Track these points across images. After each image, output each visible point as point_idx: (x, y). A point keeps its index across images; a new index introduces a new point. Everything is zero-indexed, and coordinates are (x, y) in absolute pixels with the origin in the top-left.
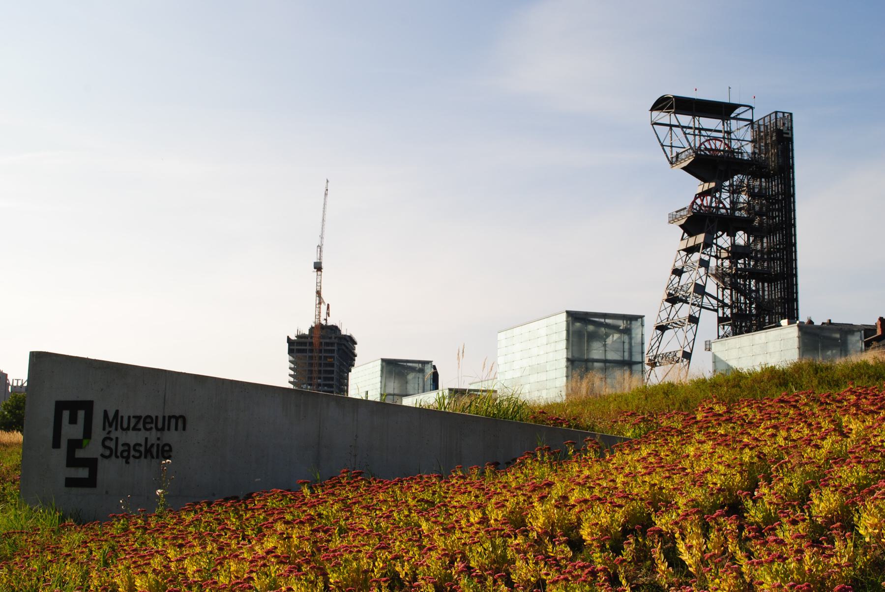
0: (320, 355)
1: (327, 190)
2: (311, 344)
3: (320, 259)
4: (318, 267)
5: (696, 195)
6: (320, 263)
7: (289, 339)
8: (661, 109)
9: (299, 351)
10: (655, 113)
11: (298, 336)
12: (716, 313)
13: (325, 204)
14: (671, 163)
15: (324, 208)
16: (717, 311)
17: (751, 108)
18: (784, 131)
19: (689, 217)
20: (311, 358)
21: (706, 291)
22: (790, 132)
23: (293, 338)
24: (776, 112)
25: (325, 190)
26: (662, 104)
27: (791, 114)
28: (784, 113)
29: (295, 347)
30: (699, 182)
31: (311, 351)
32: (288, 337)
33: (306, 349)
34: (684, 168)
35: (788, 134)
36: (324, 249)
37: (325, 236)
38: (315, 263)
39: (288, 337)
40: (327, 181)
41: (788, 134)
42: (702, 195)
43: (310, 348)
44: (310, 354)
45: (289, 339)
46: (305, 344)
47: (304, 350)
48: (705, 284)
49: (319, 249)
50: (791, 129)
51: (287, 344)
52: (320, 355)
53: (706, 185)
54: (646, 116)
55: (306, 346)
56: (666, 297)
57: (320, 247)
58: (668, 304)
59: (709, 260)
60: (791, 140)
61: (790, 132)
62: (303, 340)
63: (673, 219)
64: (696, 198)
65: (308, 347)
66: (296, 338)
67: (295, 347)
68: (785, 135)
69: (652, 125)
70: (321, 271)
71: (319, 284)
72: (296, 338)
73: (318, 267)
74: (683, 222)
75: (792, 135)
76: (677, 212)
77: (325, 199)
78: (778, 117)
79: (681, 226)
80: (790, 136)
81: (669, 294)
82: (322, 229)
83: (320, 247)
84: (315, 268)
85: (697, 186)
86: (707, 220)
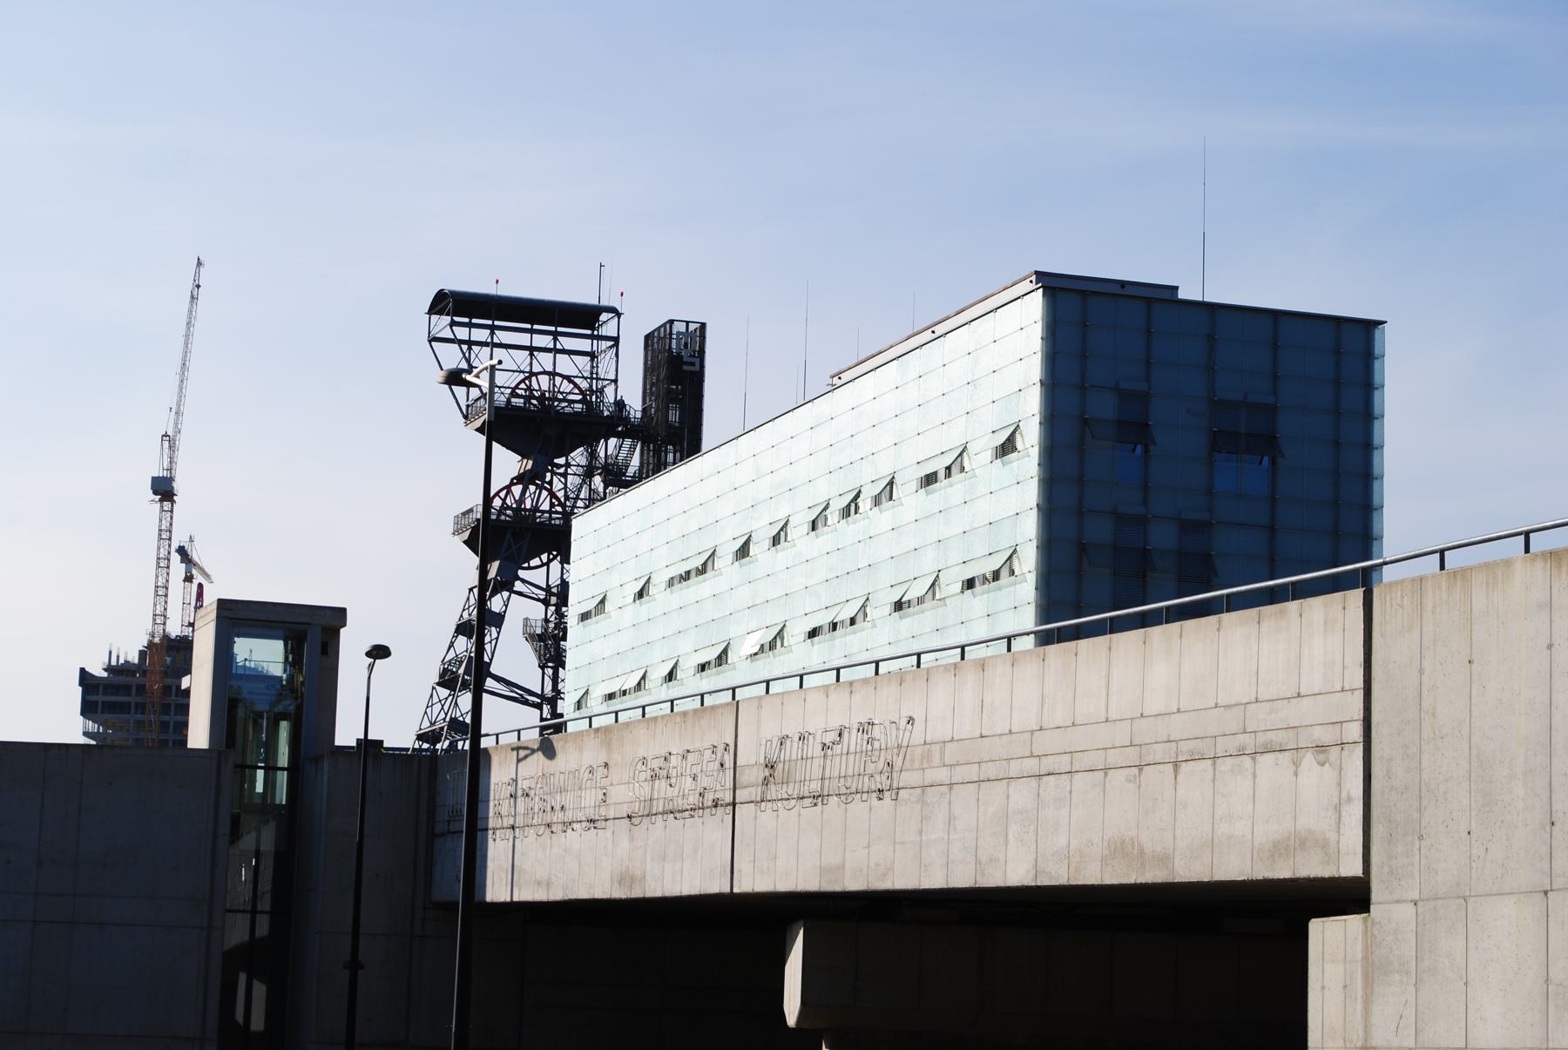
0: (166, 718)
1: (198, 286)
2: (141, 689)
3: (170, 470)
4: (164, 490)
5: (512, 479)
6: (171, 480)
7: (84, 676)
8: (440, 313)
9: (111, 707)
10: (435, 318)
11: (109, 669)
12: (539, 712)
13: (189, 324)
14: (466, 417)
15: (187, 336)
16: (539, 706)
17: (619, 315)
18: (685, 359)
19: (472, 528)
20: (140, 724)
21: (493, 670)
22: (697, 361)
23: (98, 671)
24: (671, 322)
25: (190, 285)
26: (448, 303)
27: (703, 326)
28: (687, 323)
29: (100, 698)
30: (520, 458)
31: (141, 707)
32: (83, 671)
33: (130, 703)
34: (477, 430)
35: (693, 364)
36: (183, 443)
37: (187, 410)
38: (154, 479)
39: (83, 671)
40: (199, 264)
41: (693, 364)
42: (523, 479)
43: (139, 699)
44: (139, 717)
45: (84, 676)
46: (126, 689)
47: (122, 704)
48: (491, 660)
49: (166, 444)
50: (702, 352)
51: (80, 688)
52: (166, 718)
53: (525, 461)
54: (418, 320)
55: (129, 695)
56: (437, 681)
57: (170, 440)
58: (444, 692)
59: (505, 612)
60: (698, 378)
61: (697, 361)
62: (122, 679)
63: (457, 532)
64: (512, 484)
65: (132, 699)
66: (105, 674)
67: (100, 698)
68: (685, 368)
69: (430, 341)
70: (173, 502)
71: (165, 534)
72: (105, 674)
73: (164, 490)
74: (466, 535)
75: (702, 366)
76: (464, 514)
77: (190, 312)
78: (674, 331)
79: (465, 542)
80: (697, 368)
81: (442, 675)
82: (181, 389)
83: (170, 440)
84: (155, 493)
85: (508, 464)
86: (508, 536)
